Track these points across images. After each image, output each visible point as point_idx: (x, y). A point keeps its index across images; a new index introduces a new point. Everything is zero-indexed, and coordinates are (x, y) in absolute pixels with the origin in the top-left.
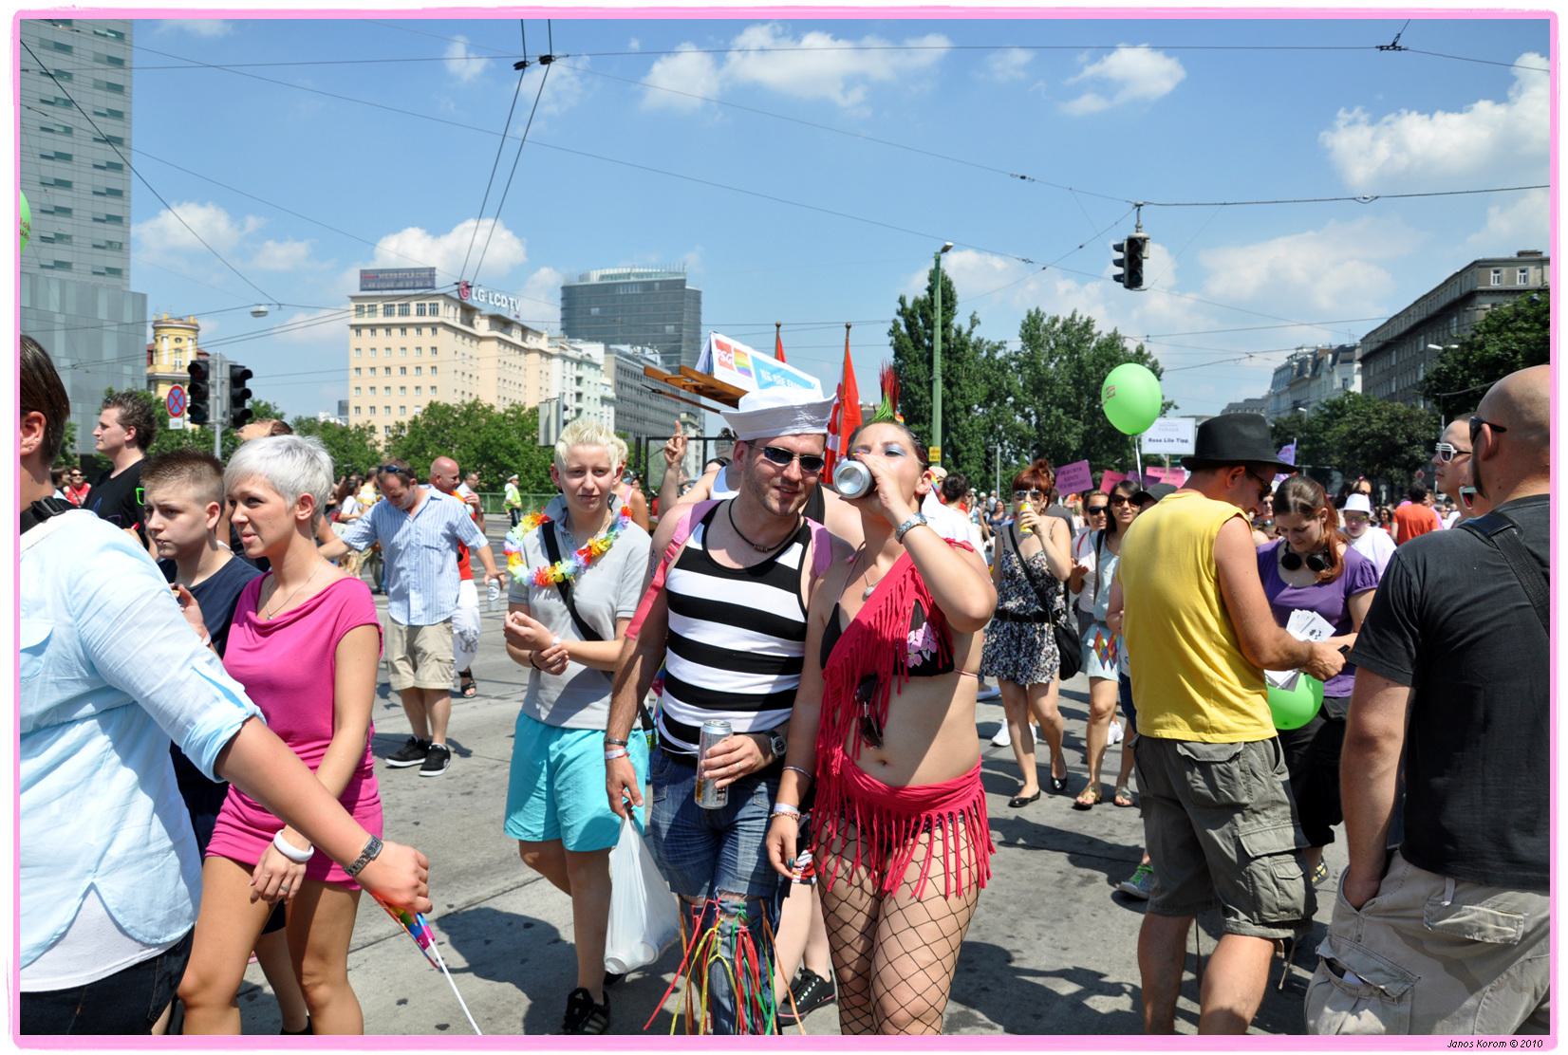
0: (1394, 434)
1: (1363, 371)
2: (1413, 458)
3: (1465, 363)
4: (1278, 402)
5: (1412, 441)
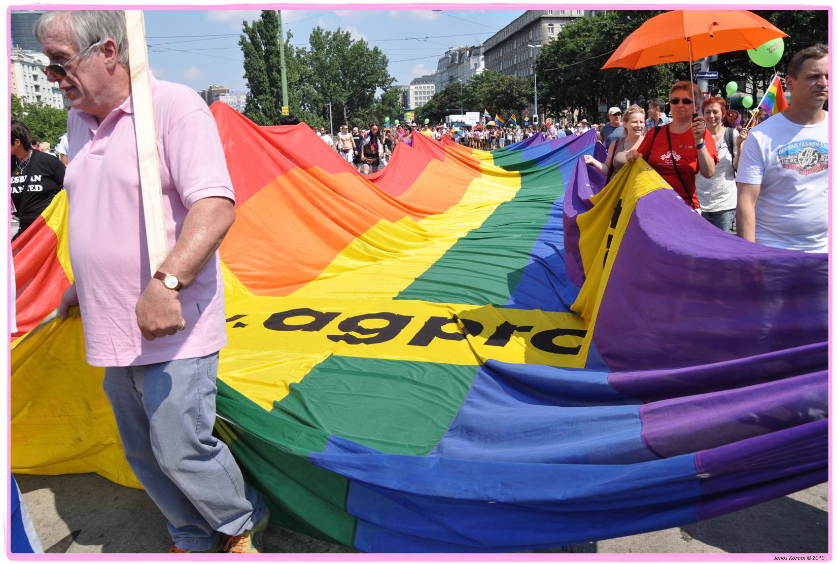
0: (512, 90)
1: (485, 59)
2: (521, 104)
3: (556, 52)
4: (442, 77)
5: (521, 95)
